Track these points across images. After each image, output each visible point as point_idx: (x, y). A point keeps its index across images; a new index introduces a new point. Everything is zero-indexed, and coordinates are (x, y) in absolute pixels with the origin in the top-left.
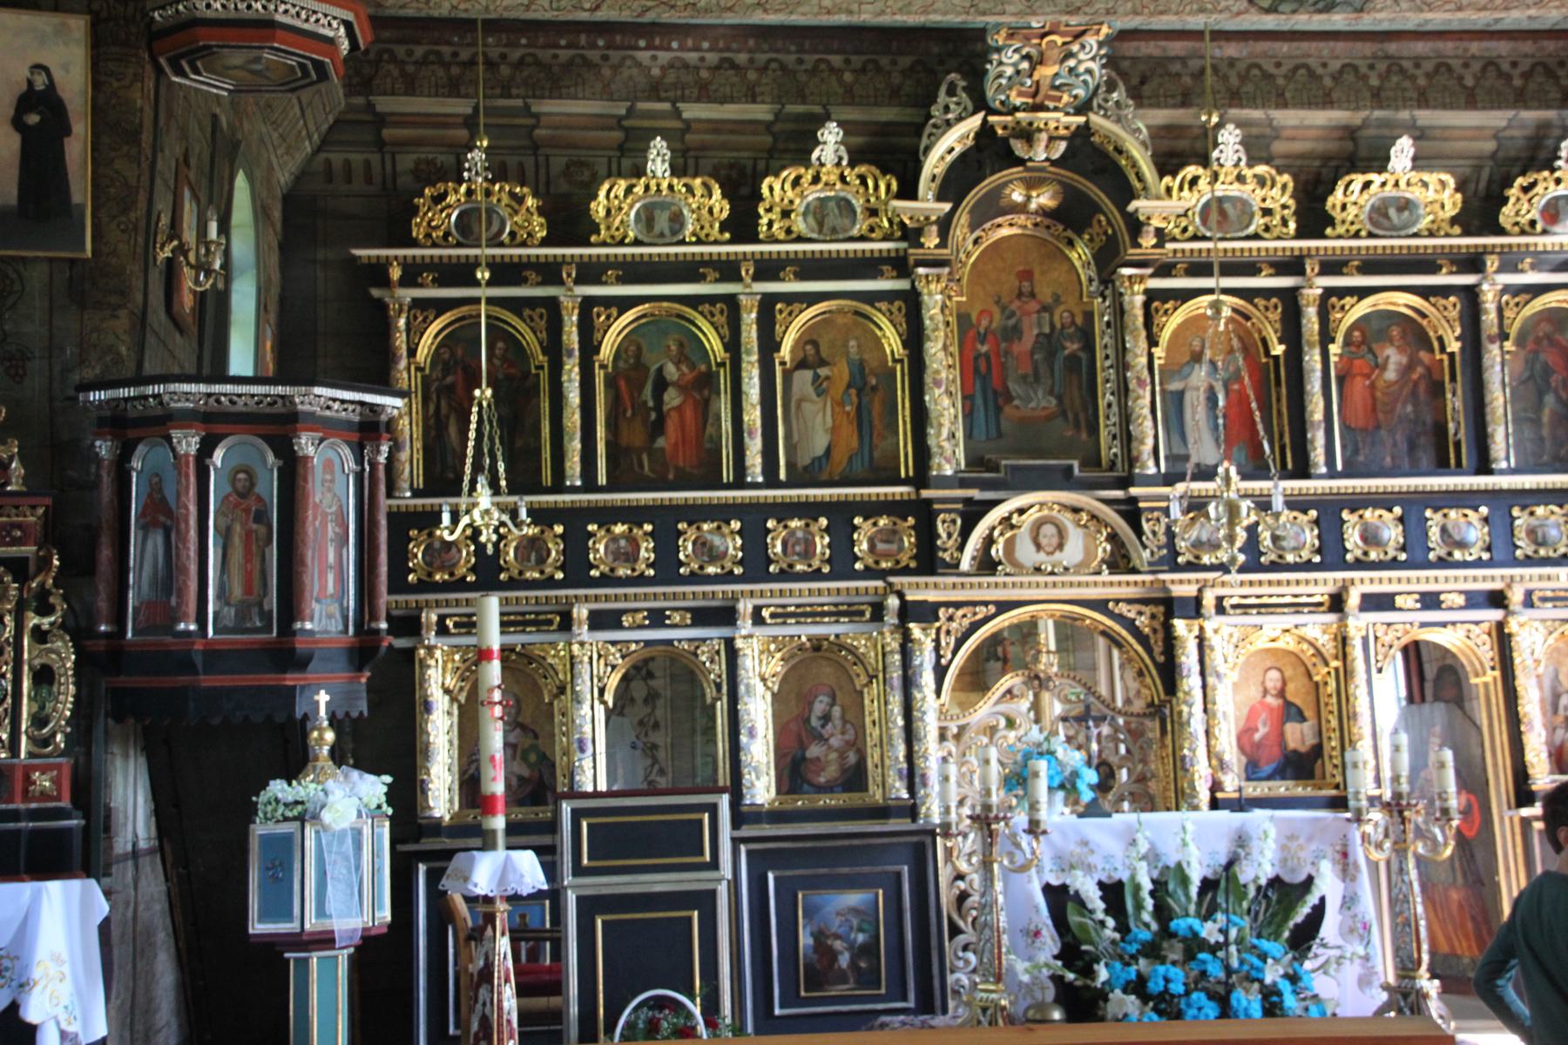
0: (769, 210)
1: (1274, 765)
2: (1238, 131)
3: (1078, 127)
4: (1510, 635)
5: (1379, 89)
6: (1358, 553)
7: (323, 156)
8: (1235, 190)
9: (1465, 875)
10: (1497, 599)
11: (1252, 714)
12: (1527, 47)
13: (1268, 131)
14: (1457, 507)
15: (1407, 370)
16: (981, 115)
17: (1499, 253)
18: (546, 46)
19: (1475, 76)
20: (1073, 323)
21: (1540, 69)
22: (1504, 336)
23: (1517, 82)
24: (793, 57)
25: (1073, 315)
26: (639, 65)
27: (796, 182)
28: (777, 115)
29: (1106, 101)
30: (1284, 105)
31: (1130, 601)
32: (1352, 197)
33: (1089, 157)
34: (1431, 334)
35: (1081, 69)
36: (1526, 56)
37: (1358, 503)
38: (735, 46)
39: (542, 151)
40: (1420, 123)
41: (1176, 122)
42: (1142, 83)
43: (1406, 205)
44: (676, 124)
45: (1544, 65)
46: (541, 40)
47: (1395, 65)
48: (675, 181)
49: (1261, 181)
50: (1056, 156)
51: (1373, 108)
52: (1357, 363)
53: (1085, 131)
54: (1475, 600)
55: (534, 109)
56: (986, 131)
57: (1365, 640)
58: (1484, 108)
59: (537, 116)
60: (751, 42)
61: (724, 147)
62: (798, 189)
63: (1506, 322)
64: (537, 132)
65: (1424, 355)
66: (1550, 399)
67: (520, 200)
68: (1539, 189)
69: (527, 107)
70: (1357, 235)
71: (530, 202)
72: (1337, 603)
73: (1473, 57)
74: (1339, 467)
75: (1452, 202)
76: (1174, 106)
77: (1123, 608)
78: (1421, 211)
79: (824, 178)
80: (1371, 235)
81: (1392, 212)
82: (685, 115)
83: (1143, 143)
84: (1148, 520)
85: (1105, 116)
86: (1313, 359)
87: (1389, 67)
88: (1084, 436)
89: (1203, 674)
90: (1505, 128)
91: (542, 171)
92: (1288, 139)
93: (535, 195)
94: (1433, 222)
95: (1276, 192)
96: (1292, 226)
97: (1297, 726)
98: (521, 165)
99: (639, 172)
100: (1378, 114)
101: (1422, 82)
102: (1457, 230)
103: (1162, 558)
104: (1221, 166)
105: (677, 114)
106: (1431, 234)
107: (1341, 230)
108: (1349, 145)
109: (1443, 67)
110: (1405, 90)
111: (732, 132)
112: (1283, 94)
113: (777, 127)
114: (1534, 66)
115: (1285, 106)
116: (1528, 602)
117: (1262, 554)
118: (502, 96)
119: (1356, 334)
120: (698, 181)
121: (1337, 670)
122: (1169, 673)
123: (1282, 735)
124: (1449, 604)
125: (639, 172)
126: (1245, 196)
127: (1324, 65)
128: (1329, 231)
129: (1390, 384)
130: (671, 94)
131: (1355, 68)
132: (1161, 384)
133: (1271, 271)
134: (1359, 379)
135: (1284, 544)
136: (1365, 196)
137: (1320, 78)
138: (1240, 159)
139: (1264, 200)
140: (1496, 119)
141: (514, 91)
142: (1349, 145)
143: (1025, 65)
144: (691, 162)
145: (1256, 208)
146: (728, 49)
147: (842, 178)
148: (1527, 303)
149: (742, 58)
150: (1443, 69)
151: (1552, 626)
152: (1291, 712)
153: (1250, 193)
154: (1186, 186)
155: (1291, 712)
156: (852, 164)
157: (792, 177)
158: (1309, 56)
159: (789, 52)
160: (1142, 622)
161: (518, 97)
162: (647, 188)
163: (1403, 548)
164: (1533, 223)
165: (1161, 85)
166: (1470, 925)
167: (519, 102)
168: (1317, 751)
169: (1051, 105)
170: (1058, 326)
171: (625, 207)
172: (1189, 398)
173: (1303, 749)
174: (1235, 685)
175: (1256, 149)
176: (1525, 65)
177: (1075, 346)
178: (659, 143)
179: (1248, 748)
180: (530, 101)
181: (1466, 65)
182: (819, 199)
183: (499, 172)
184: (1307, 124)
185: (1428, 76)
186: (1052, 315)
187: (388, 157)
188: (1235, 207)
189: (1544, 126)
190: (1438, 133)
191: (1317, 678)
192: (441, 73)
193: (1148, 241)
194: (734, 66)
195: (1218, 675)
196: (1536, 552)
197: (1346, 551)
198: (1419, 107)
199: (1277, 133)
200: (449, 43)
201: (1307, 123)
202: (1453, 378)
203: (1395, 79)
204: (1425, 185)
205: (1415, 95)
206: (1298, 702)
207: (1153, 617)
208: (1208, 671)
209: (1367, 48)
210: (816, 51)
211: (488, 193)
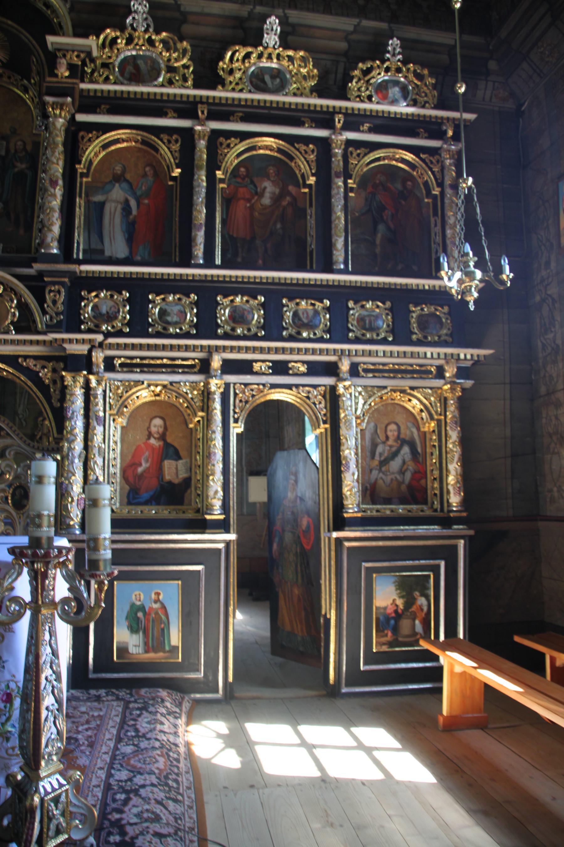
1: (152, 493)
4: (339, 396)
6: (228, 328)
9: (302, 577)
10: (331, 369)
11: (137, 453)
14: (307, 298)
15: (277, 199)
17: (343, 114)
20: (25, 149)
22: (347, 175)
25: (25, 144)
31: (35, 358)
34: (297, 172)
37: (230, 288)
40: (291, 20)
43: (277, 74)
52: (241, 190)
54: (315, 369)
57: (225, 397)
58: (337, 14)
63: (351, 166)
65: (291, 188)
66: (381, 228)
68: (374, 73)
72: (204, 367)
74: (218, 261)
77: (31, 363)
81: (267, 78)
84: (50, 291)
86: (202, 178)
88: (22, 232)
89: (87, 416)
90: (352, 33)
92: (193, 23)
96: (190, 83)
97: (173, 463)
103: (60, 323)
116: (354, 371)
117: (150, 325)
119: (242, 169)
121: (202, 417)
122: (61, 417)
123: (160, 469)
124: (296, 371)
129: (265, 207)
132: (87, 195)
133: (176, 115)
134: (242, 202)
135: (169, 319)
138: (148, 26)
140: (345, 24)
145: (163, 66)
148: (366, 155)
151: (369, 391)
152: (170, 451)
155: (170, 451)
160: (45, 374)
163: (263, 327)
166: (303, 614)
168: (187, 482)
170: (13, 151)
172: (108, 208)
173: (176, 481)
174: (123, 428)
177: (24, 166)
179: (131, 479)
186: (8, 143)
188: (146, 64)
191: (191, 426)
193: (63, 72)
195: (97, 418)
196: (364, 335)
197: (218, 326)
198: (290, 7)
201: (207, 10)
202: (311, 205)
204: (291, 59)
206: (176, 444)
207: (54, 371)
208: (91, 414)
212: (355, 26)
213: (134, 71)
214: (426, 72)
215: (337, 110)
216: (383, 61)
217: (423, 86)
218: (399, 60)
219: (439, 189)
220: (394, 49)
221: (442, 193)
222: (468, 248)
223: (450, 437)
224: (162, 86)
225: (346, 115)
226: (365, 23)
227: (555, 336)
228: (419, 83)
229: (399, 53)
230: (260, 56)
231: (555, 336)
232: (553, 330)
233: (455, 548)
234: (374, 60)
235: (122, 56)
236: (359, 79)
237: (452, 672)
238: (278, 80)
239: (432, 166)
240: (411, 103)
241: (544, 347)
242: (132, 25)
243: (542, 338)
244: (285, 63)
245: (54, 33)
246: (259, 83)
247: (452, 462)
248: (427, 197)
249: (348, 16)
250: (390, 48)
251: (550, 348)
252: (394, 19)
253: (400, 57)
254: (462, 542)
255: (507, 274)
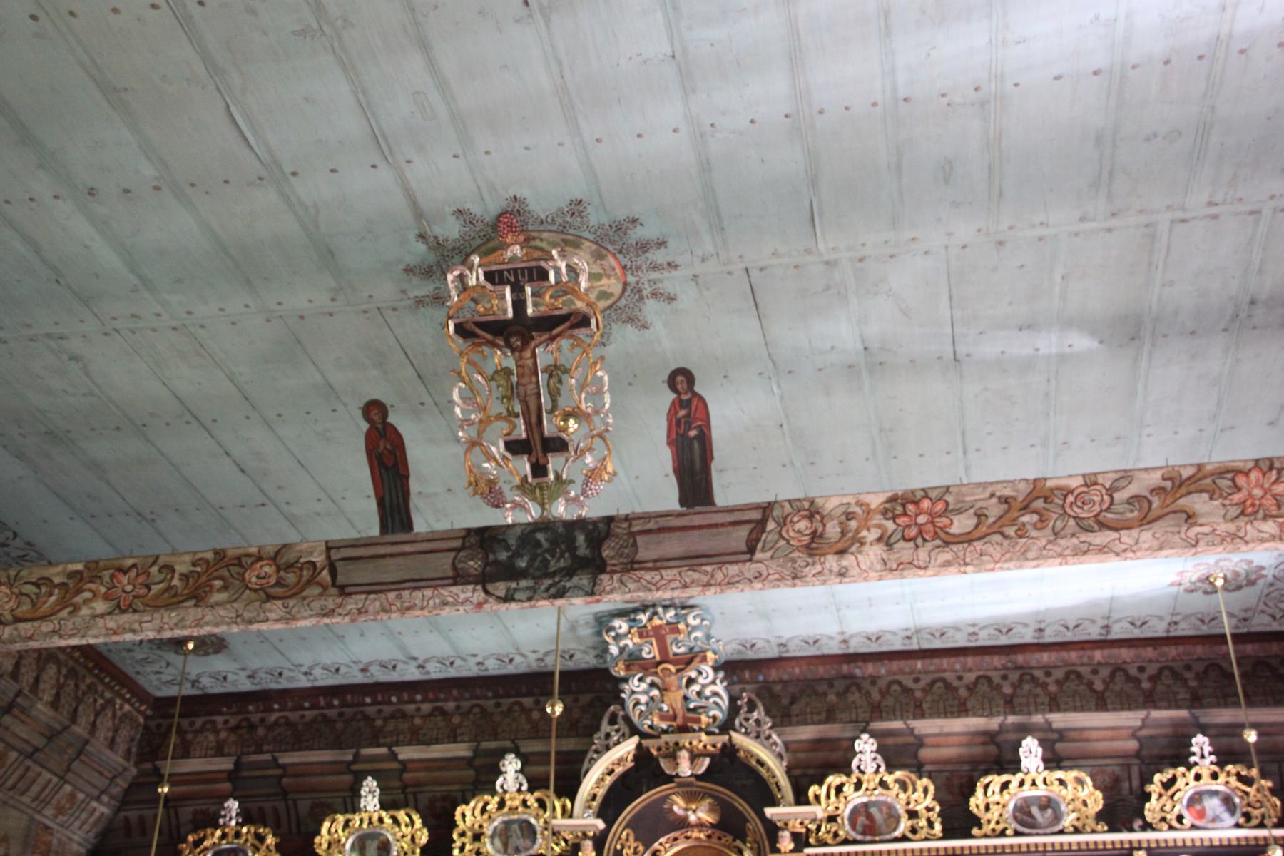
0: (463, 834)
2: (872, 740)
3: (724, 745)
5: (1012, 696)
7: (122, 814)
8: (879, 794)
12: (1149, 652)
13: (911, 740)
16: (636, 739)
18: (294, 709)
19: (1104, 681)
21: (1166, 673)
23: (1146, 685)
24: (492, 702)
26: (366, 718)
27: (484, 810)
28: (476, 751)
29: (747, 720)
30: (922, 715)
32: (993, 798)
33: (730, 771)
35: (707, 692)
36: (1151, 661)
38: (442, 696)
39: (289, 797)
40: (1055, 726)
41: (823, 735)
42: (792, 703)
43: (1047, 804)
44: (395, 765)
45: (1171, 669)
46: (290, 704)
47: (1026, 674)
48: (384, 814)
49: (903, 786)
50: (701, 771)
51: (1005, 714)
53: (730, 751)
55: (281, 761)
56: (642, 755)
58: (1114, 710)
59: (284, 767)
60: (455, 692)
61: (437, 782)
62: (486, 816)
64: (285, 780)
67: (261, 838)
68: (1180, 783)
69: (275, 759)
70: (1002, 834)
71: (270, 840)
73: (1099, 663)
75: (1096, 800)
76: (820, 722)
78: (1063, 807)
79: (509, 803)
80: (1017, 834)
81: (1035, 810)
82: (401, 757)
83: (780, 756)
85: (747, 734)
87: (1022, 676)
90: (1141, 728)
91: (293, 812)
92: (933, 746)
93: (274, 835)
94: (1078, 819)
95: (919, 794)
96: (938, 827)
98: (276, 810)
99: (355, 809)
100: (1011, 719)
101: (1053, 688)
102: (1102, 826)
104: (863, 773)
105: (394, 756)
106: (1077, 831)
107: (987, 829)
108: (992, 749)
109: (1072, 674)
110: (1037, 696)
111: (441, 769)
112: (920, 706)
113: (478, 762)
114: (1161, 670)
115: (923, 716)
118: (255, 753)
120: (401, 815)
125: (355, 809)
126: (889, 800)
127: (960, 678)
128: (975, 831)
130: (388, 740)
131: (989, 679)
136: (1006, 796)
137: (956, 689)
138: (879, 766)
139: (908, 803)
140: (1130, 719)
141: (265, 748)
142: (992, 749)
143: (655, 692)
144: (411, 798)
145: (901, 811)
146: (437, 700)
147: (524, 802)
149: (450, 705)
150: (1073, 676)
153: (897, 799)
154: (833, 792)
156: (531, 790)
157: (480, 805)
158: (945, 671)
159: (486, 698)
161: (267, 752)
162: (361, 821)
164: (1180, 818)
165: (808, 704)
167: (267, 757)
169: (696, 727)
171: (343, 840)
175: (898, 755)
176: (1152, 669)
178: (370, 783)
180: (277, 754)
181: (1095, 672)
182: (504, 822)
183: (247, 817)
184: (948, 732)
185: (1058, 682)
187: (172, 811)
188: (881, 811)
189: (1176, 724)
190: (1073, 735)
192: (212, 737)
194: (443, 712)
198: (1051, 711)
199: (920, 742)
200: (221, 714)
201: (946, 730)
203: (1026, 687)
204: (1062, 782)
205: (1047, 701)
209: (997, 661)
210: (509, 696)
211: (238, 835)
212: (1143, 720)
213: (867, 822)
215: (1136, 845)
216: (1189, 767)
218: (1212, 763)
224: (904, 839)
225: (1148, 849)
226: (1156, 714)
229: (1210, 754)
230: (1022, 783)
234: (1175, 766)
235: (850, 806)
236: (1161, 795)
238: (1049, 811)
240: (1242, 820)
242: (859, 767)
244: (1056, 787)
245: (774, 803)
246: (1025, 818)
249: (1130, 709)
250: (1194, 749)
252: (1196, 701)
253: (1213, 758)
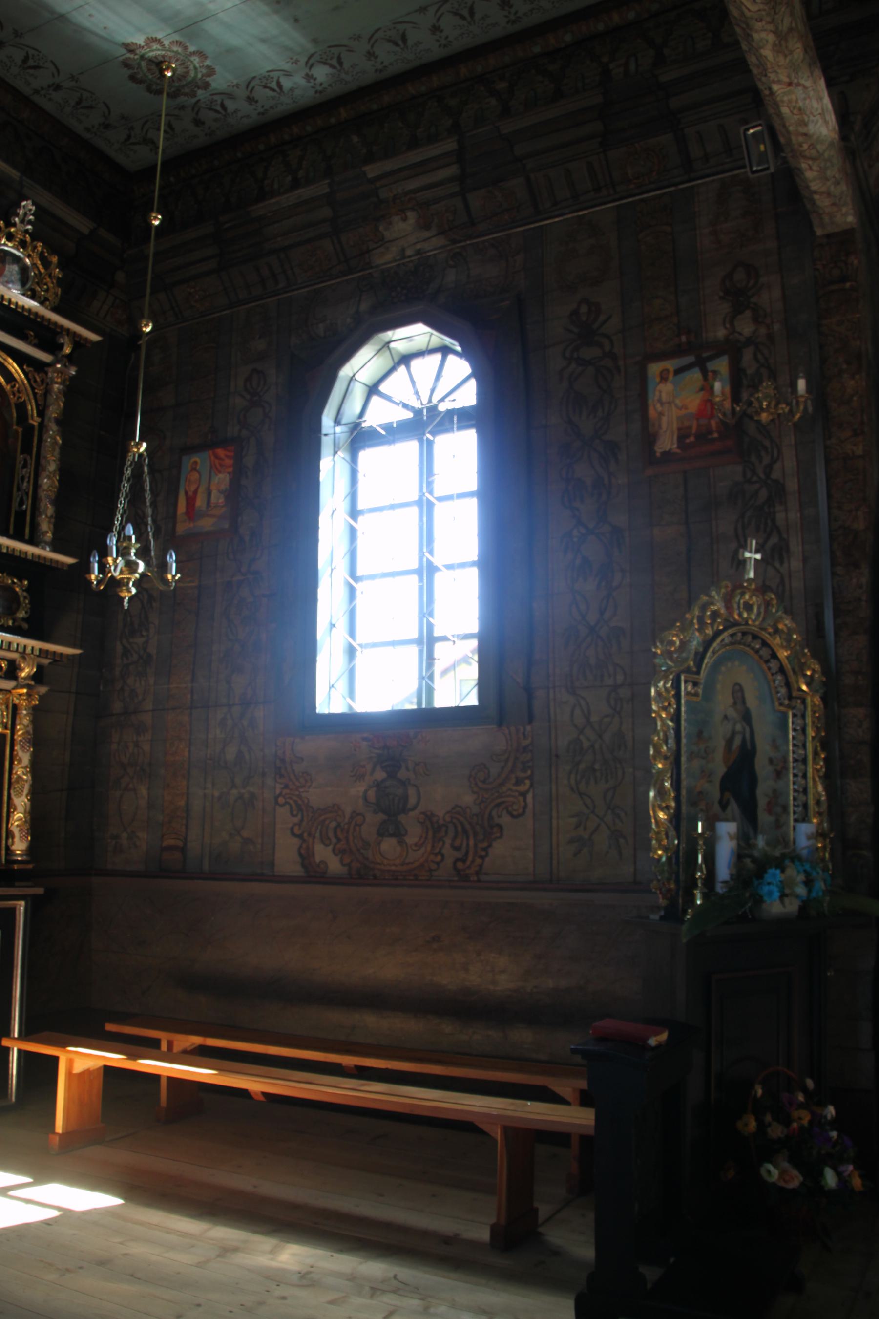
214: (55, 259)
217: (47, 277)
218: (27, 231)
219: (39, 420)
220: (25, 214)
221: (42, 425)
222: (130, 530)
223: (20, 761)
227: (147, 642)
228: (43, 271)
229: (30, 222)
231: (147, 642)
232: (144, 633)
233: (13, 911)
237: (69, 1074)
239: (34, 385)
241: (126, 652)
243: (124, 641)
247: (19, 794)
248: (18, 424)
251: (135, 657)
254: (23, 903)
255: (173, 574)
